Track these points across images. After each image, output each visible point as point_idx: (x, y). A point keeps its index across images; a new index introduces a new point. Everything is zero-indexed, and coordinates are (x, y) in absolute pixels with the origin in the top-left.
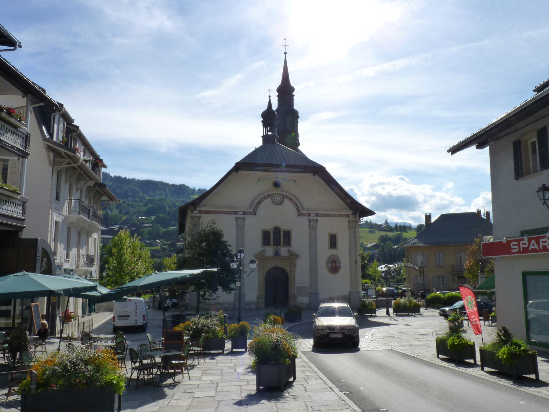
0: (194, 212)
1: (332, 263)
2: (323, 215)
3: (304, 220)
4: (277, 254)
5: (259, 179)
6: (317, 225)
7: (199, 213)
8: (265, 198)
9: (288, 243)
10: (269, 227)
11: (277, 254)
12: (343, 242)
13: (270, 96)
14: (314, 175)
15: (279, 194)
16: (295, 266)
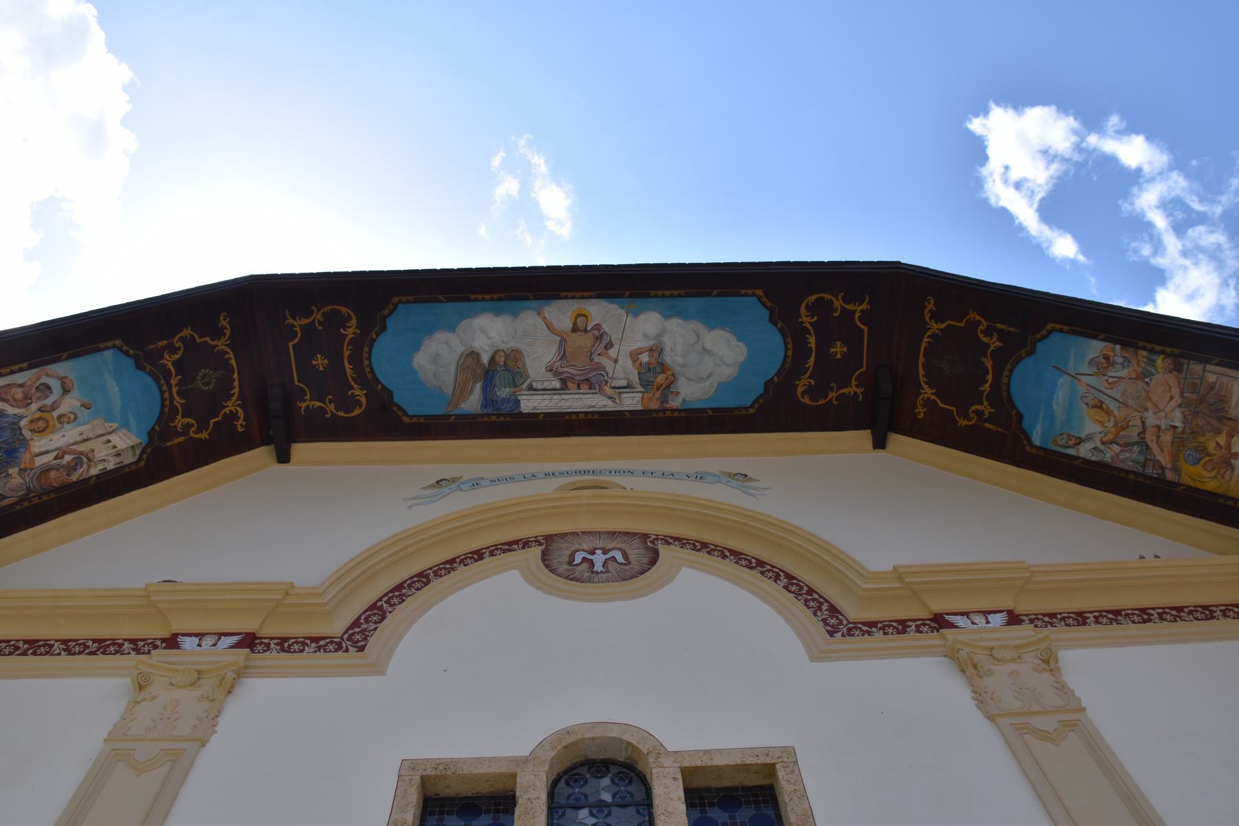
3: (918, 680)
6: (1063, 689)
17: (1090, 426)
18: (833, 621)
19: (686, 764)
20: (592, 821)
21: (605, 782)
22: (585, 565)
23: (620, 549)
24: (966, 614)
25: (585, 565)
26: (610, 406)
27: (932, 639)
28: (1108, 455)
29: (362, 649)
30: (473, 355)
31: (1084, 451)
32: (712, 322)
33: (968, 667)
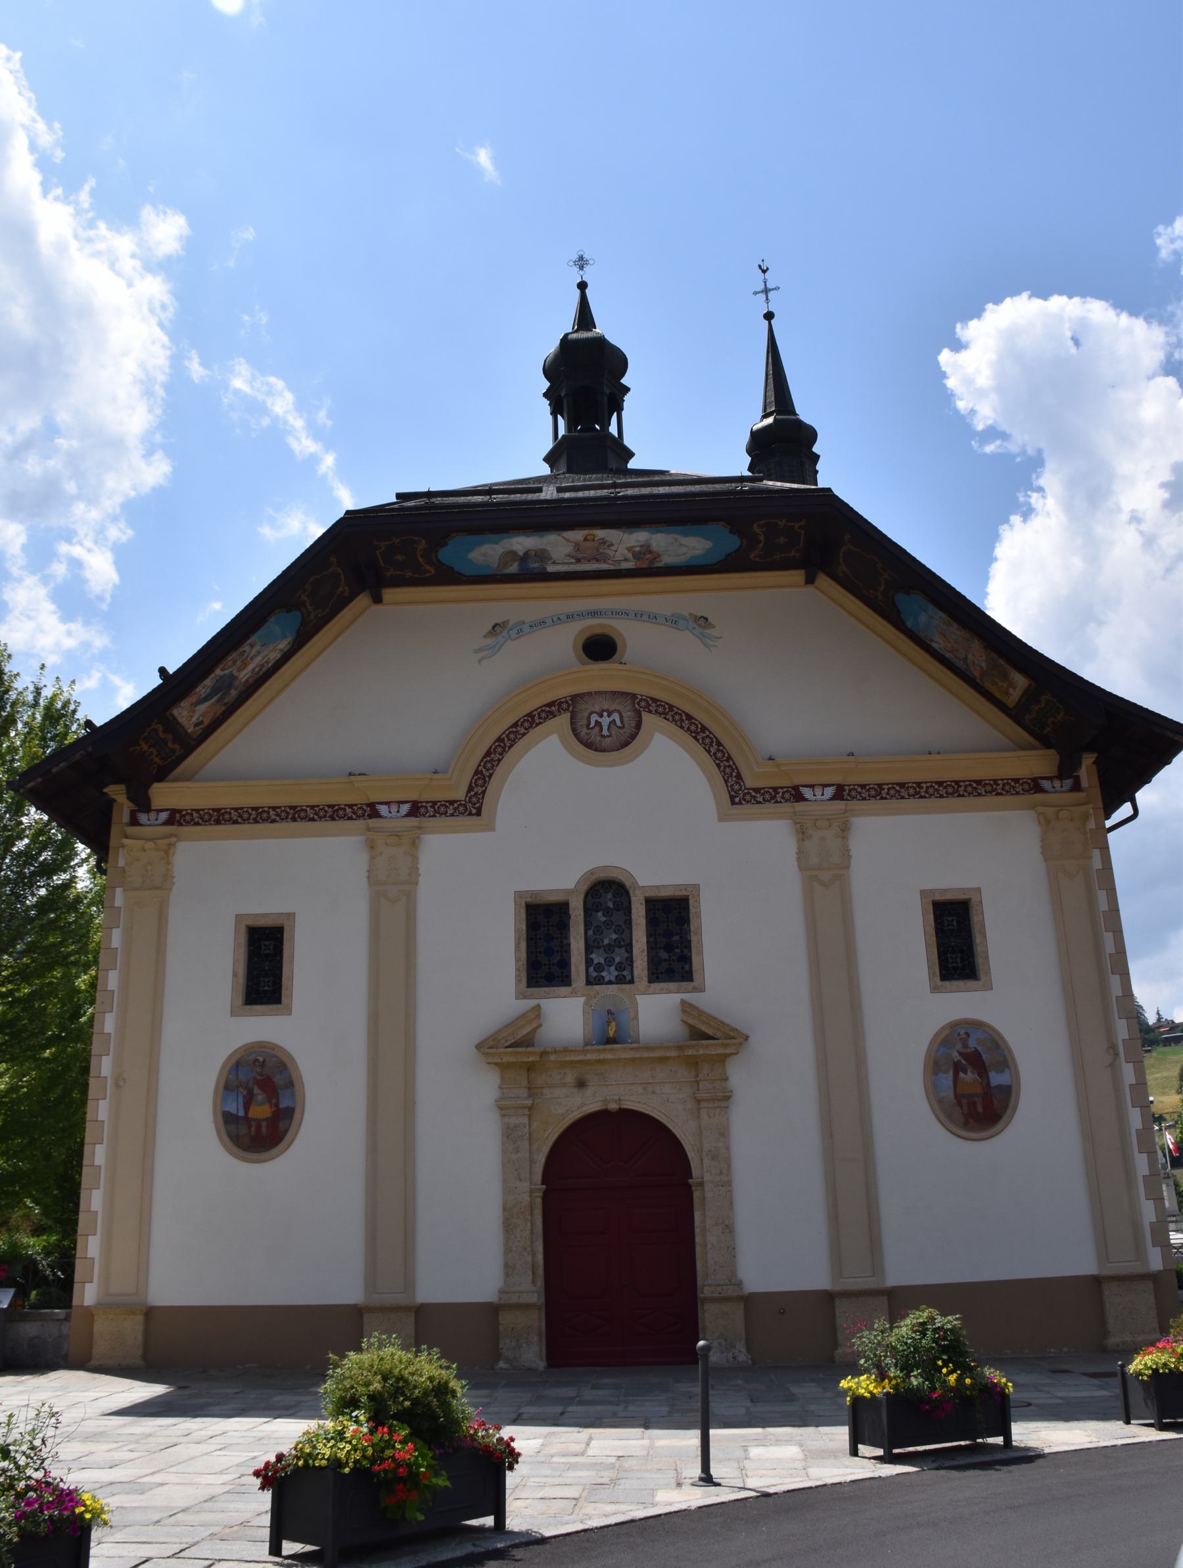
0: (143, 817)
1: (957, 1068)
2: (878, 792)
4: (611, 1034)
5: (496, 629)
6: (846, 853)
7: (169, 822)
8: (531, 721)
9: (674, 959)
10: (562, 878)
11: (611, 1034)
12: (1015, 936)
13: (582, 286)
14: (810, 581)
15: (615, 694)
16: (726, 1098)
17: (937, 638)
18: (736, 787)
19: (647, 895)
20: (604, 919)
21: (610, 895)
22: (597, 728)
23: (620, 714)
24: (812, 786)
25: (597, 728)
26: (612, 567)
27: (787, 807)
28: (947, 655)
29: (479, 814)
30: (514, 553)
31: (934, 645)
32: (686, 535)
33: (802, 834)
